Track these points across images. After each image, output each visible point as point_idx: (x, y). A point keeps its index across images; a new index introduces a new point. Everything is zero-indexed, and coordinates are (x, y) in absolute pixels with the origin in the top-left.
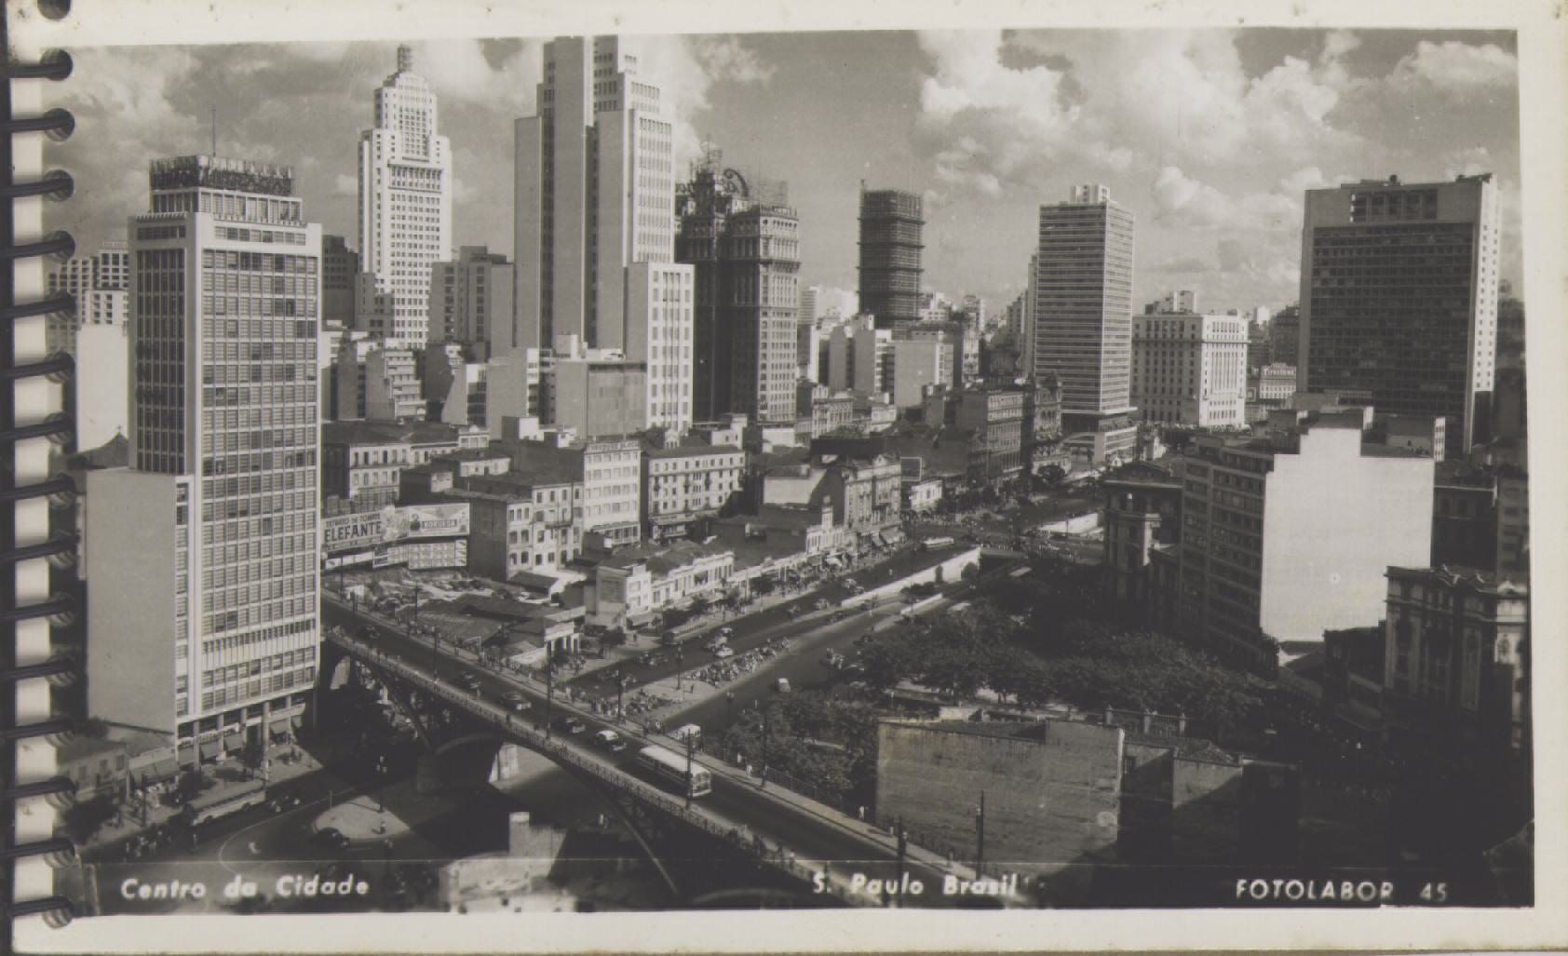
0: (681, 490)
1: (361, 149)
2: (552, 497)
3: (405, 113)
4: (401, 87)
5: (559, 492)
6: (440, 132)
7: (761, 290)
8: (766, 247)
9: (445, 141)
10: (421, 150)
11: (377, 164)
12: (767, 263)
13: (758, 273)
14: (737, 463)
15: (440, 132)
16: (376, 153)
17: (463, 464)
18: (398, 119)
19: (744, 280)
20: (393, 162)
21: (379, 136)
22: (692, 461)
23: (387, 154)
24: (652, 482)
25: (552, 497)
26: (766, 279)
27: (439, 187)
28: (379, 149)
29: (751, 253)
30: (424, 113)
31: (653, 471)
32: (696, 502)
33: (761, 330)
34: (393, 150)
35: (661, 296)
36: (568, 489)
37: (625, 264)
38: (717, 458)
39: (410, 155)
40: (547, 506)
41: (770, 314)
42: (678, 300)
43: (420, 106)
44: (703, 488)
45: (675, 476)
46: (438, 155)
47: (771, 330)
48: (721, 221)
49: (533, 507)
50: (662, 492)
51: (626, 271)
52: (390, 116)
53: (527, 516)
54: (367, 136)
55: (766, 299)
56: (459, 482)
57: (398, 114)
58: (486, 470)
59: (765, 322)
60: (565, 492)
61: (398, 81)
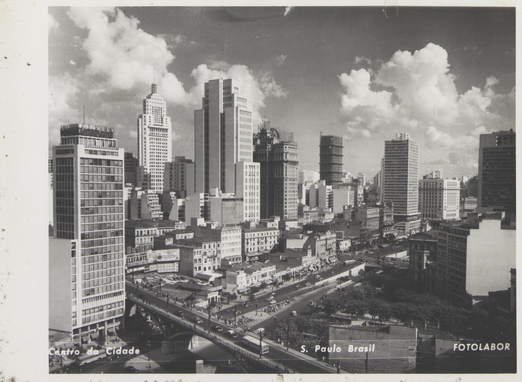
1: (138, 121)
2: (209, 247)
3: (154, 108)
4: (153, 99)
9: (169, 119)
11: (144, 127)
13: (283, 165)
16: (144, 123)
18: (152, 110)
19: (278, 168)
20: (150, 126)
23: (148, 123)
24: (246, 240)
25: (209, 247)
26: (286, 167)
27: (167, 135)
28: (145, 121)
29: (281, 159)
30: (161, 108)
31: (246, 237)
34: (150, 121)
37: (235, 163)
39: (156, 124)
42: (254, 176)
43: (160, 106)
44: (264, 243)
45: (254, 239)
46: (167, 123)
47: (288, 186)
48: (270, 147)
50: (249, 244)
52: (149, 109)
53: (200, 254)
54: (141, 117)
55: (286, 175)
57: (152, 108)
60: (214, 244)
61: (152, 97)
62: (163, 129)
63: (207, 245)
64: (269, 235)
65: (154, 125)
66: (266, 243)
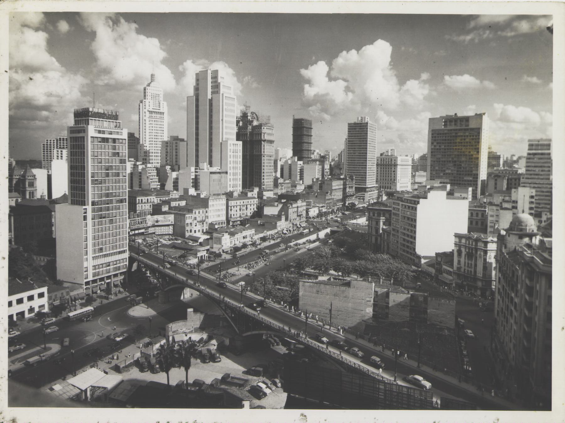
0: (238, 210)
1: (139, 106)
2: (199, 213)
5: (201, 211)
6: (164, 101)
7: (263, 149)
9: (165, 103)
10: (158, 106)
11: (144, 110)
12: (264, 141)
13: (262, 144)
14: (255, 202)
15: (164, 101)
16: (144, 107)
17: (171, 203)
20: (149, 110)
22: (242, 201)
23: (147, 107)
24: (230, 208)
25: (199, 213)
26: (264, 145)
31: (230, 205)
32: (243, 214)
33: (263, 161)
35: (232, 151)
36: (204, 210)
37: (221, 141)
38: (249, 200)
41: (265, 156)
45: (236, 206)
47: (265, 161)
49: (193, 216)
51: (221, 143)
52: (149, 96)
54: (141, 102)
55: (264, 152)
56: (170, 208)
58: (179, 204)
63: (197, 211)
64: (249, 203)
66: (247, 210)
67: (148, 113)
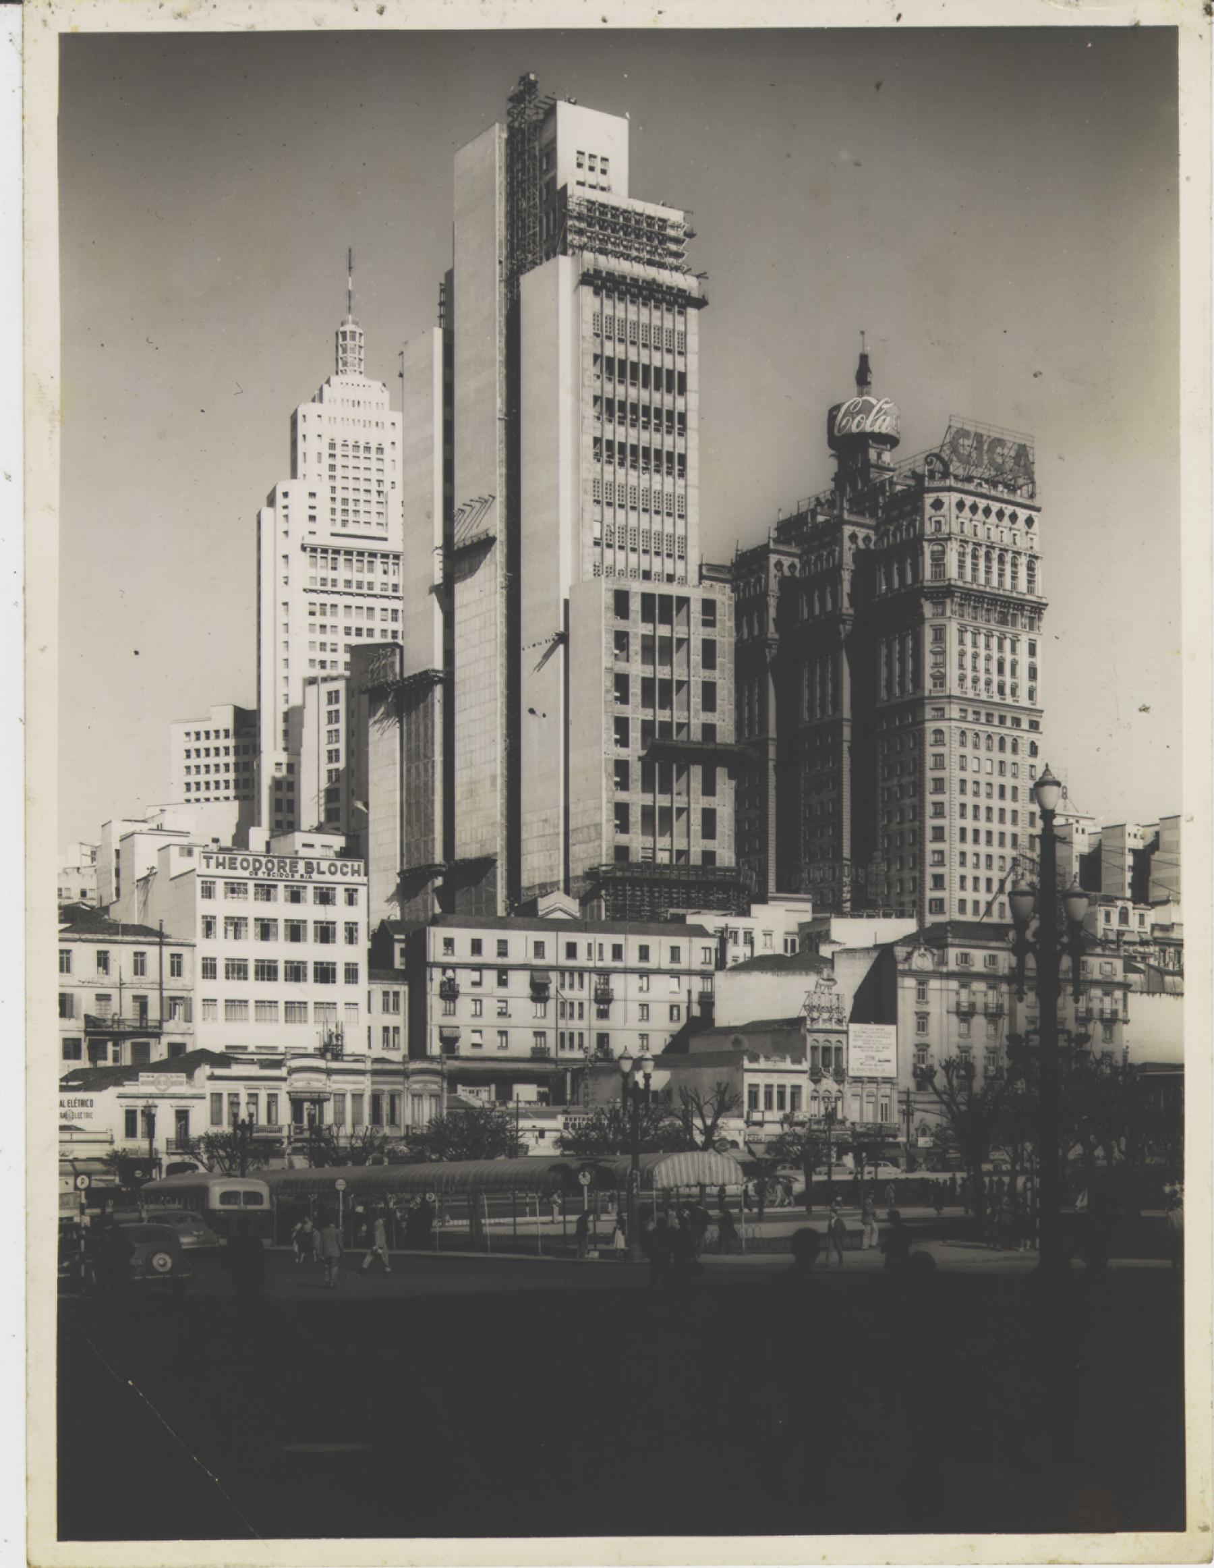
3: (339, 451)
7: (929, 659)
8: (939, 560)
10: (374, 518)
13: (921, 620)
18: (327, 461)
20: (311, 541)
21: (286, 495)
24: (437, 976)
28: (286, 516)
29: (909, 580)
30: (380, 450)
31: (436, 951)
32: (565, 1039)
34: (312, 518)
37: (565, 594)
39: (351, 529)
40: (83, 984)
41: (954, 711)
43: (373, 437)
44: (591, 1009)
48: (861, 533)
50: (464, 1005)
51: (566, 602)
52: (312, 457)
55: (940, 680)
57: (326, 451)
59: (938, 732)
62: (385, 556)
64: (631, 958)
65: (333, 535)
67: (305, 557)
